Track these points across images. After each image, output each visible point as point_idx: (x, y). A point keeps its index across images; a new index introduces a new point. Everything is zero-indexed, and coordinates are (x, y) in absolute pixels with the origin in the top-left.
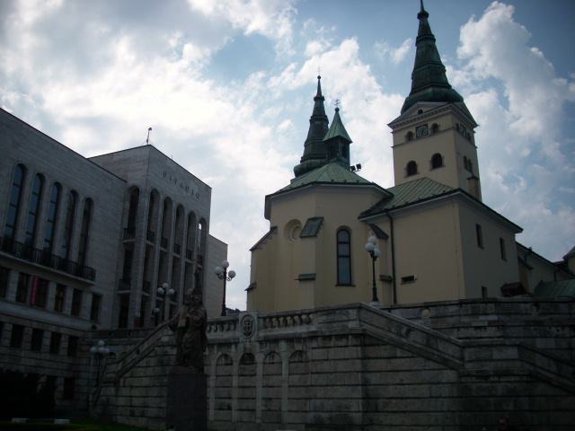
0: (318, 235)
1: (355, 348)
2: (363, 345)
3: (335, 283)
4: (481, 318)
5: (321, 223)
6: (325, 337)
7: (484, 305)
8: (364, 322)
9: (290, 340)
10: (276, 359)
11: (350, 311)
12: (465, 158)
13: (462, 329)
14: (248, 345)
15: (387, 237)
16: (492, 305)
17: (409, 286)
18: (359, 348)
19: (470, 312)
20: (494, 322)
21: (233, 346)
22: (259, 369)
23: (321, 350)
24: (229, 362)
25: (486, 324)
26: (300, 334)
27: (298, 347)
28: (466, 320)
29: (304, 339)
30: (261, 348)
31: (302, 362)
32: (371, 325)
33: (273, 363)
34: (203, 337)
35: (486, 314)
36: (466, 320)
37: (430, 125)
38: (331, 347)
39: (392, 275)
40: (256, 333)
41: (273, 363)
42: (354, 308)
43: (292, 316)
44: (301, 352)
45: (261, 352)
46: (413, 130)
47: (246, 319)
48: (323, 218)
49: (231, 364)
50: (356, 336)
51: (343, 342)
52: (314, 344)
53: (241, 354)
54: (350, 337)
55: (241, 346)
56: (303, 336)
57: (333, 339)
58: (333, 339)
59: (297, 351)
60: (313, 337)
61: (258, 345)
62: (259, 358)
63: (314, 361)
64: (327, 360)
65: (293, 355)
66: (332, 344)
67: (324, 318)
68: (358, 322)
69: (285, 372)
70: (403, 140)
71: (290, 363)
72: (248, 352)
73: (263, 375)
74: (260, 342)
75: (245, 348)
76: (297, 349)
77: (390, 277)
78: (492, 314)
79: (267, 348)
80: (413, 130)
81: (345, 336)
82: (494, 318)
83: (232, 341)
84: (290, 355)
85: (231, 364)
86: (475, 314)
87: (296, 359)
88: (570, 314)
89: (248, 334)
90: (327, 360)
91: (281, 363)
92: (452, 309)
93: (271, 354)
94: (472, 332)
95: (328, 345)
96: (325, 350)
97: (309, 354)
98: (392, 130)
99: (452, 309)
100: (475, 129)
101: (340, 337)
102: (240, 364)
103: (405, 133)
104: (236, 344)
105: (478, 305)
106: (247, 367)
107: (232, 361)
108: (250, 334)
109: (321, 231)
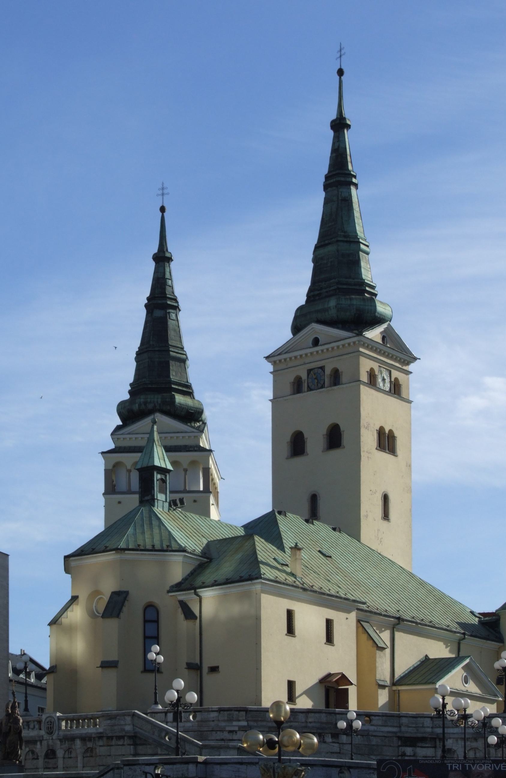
0: (122, 615)
1: (129, 747)
2: (135, 745)
3: (141, 668)
4: (235, 723)
5: (125, 599)
6: (110, 738)
7: (237, 712)
8: (137, 727)
9: (84, 739)
10: (73, 755)
11: (126, 717)
12: (381, 432)
13: (219, 732)
14: (51, 742)
15: (195, 617)
16: (243, 713)
17: (214, 676)
18: (132, 747)
19: (226, 718)
20: (244, 726)
21: (38, 743)
22: (60, 762)
23: (105, 748)
24: (36, 758)
25: (236, 729)
26: (92, 733)
27: (90, 745)
28: (223, 724)
29: (94, 738)
30: (61, 745)
31: (92, 756)
32: (141, 729)
33: (71, 758)
34: (20, 738)
35: (239, 721)
36: (223, 724)
37: (328, 371)
38: (112, 745)
39: (199, 664)
40: (57, 732)
41: (71, 758)
42: (129, 715)
43: (84, 720)
44: (91, 750)
45: (61, 748)
46: (304, 376)
47: (48, 720)
48: (127, 593)
49: (38, 759)
50: (130, 737)
51: (121, 742)
52: (101, 743)
53: (46, 750)
54: (126, 738)
55: (45, 743)
56: (93, 736)
57: (114, 739)
58: (114, 739)
59: (89, 748)
60: (100, 737)
61: (58, 742)
62: (60, 753)
63: (100, 756)
64: (110, 755)
65: (86, 751)
66: (114, 742)
67: (109, 722)
68: (132, 726)
69: (80, 765)
70: (288, 389)
71: (84, 757)
72: (51, 748)
73: (64, 768)
74: (61, 740)
75: (48, 746)
76: (88, 746)
77: (197, 664)
78: (243, 720)
79: (66, 745)
80: (304, 376)
81: (122, 737)
82: (244, 723)
83: (37, 739)
84: (83, 750)
85: (38, 759)
86: (230, 720)
87: (88, 755)
88: (306, 722)
89: (50, 733)
90: (110, 755)
91: (77, 757)
92: (214, 715)
93: (69, 750)
94: (226, 735)
95: (111, 744)
96: (109, 747)
97: (97, 751)
98: (270, 367)
99: (214, 715)
100: (411, 367)
101: (119, 738)
102: (44, 759)
103: (291, 377)
104: (41, 741)
105: (233, 712)
106: (50, 761)
107: (38, 756)
108: (52, 733)
109: (124, 609)
